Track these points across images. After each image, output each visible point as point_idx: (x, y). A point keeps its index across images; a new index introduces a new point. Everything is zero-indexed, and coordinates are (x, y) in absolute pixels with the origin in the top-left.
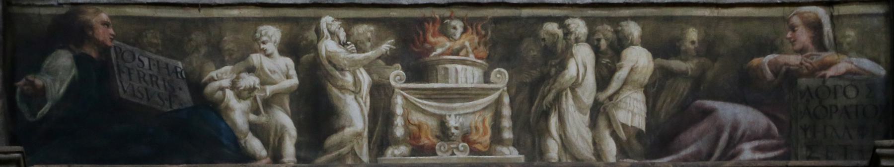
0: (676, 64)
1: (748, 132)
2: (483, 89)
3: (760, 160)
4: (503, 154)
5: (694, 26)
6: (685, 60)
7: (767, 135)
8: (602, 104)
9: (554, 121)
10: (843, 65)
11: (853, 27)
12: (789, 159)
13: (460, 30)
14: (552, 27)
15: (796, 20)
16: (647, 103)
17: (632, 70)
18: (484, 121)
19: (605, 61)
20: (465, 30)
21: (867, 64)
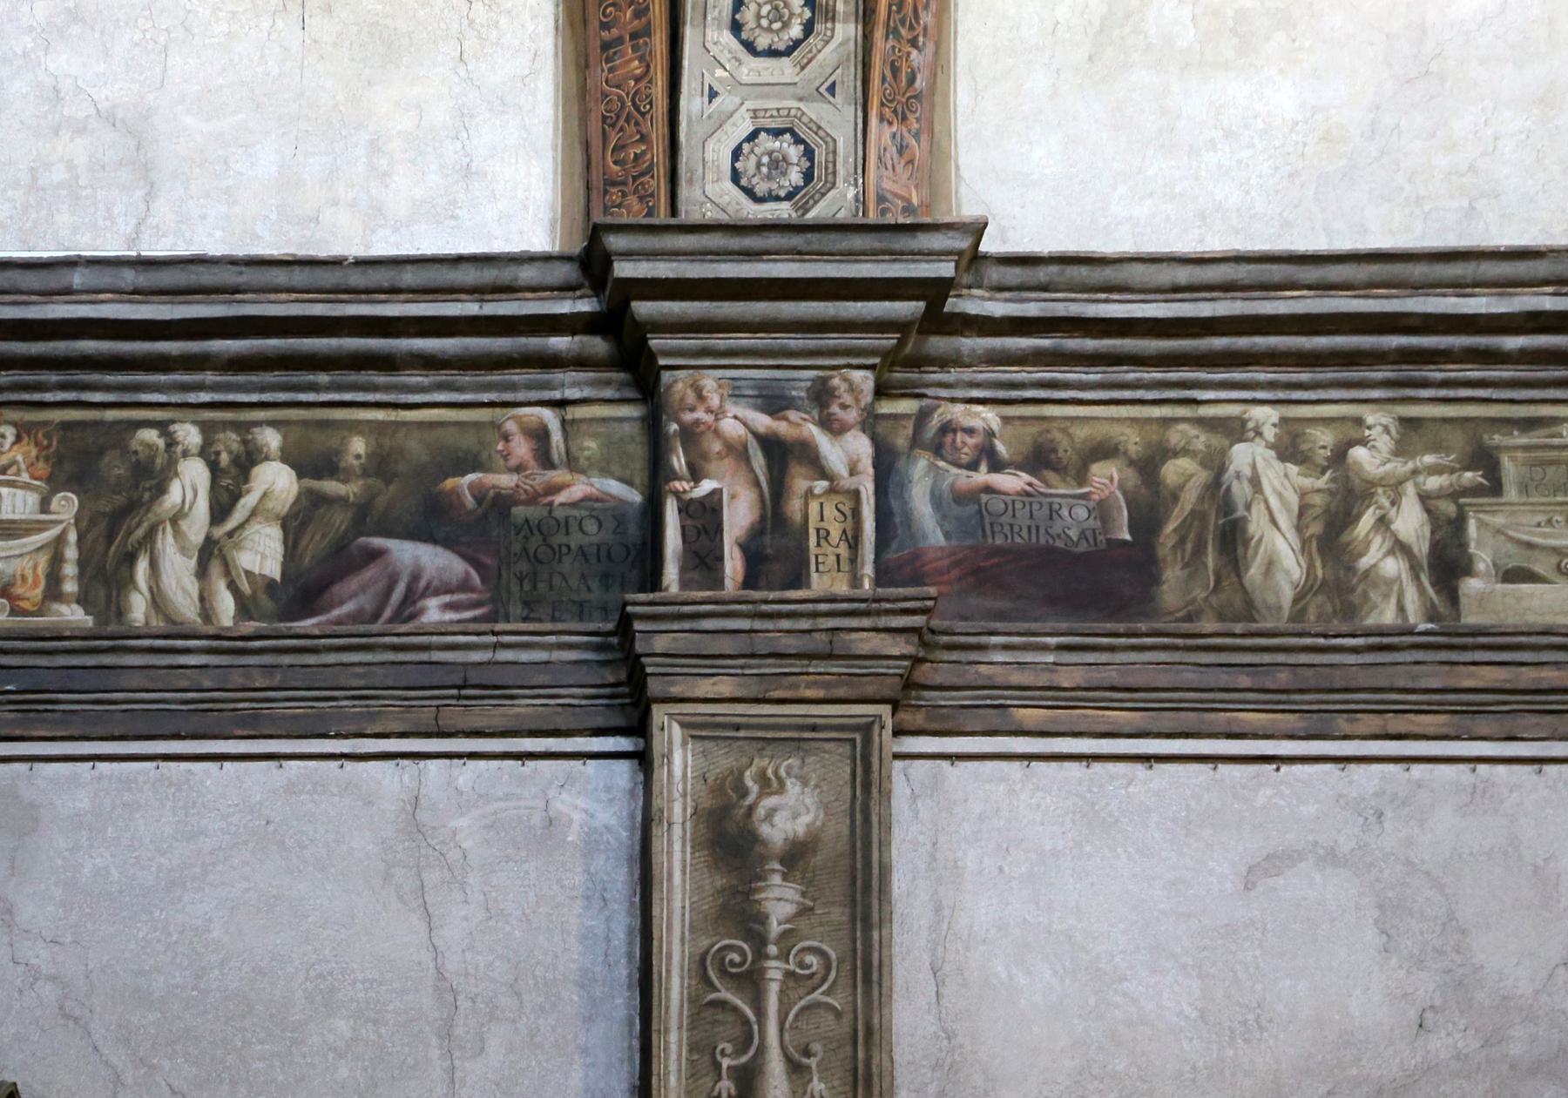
0: (331, 486)
1: (436, 583)
2: (38, 522)
3: (452, 622)
4: (61, 615)
5: (361, 433)
6: (345, 482)
7: (464, 586)
8: (216, 542)
9: (142, 567)
10: (579, 488)
11: (594, 436)
12: (496, 621)
13: (10, 438)
14: (150, 435)
15: (511, 426)
16: (285, 542)
17: (265, 494)
18: (35, 568)
19: (225, 482)
20: (18, 439)
21: (614, 487)
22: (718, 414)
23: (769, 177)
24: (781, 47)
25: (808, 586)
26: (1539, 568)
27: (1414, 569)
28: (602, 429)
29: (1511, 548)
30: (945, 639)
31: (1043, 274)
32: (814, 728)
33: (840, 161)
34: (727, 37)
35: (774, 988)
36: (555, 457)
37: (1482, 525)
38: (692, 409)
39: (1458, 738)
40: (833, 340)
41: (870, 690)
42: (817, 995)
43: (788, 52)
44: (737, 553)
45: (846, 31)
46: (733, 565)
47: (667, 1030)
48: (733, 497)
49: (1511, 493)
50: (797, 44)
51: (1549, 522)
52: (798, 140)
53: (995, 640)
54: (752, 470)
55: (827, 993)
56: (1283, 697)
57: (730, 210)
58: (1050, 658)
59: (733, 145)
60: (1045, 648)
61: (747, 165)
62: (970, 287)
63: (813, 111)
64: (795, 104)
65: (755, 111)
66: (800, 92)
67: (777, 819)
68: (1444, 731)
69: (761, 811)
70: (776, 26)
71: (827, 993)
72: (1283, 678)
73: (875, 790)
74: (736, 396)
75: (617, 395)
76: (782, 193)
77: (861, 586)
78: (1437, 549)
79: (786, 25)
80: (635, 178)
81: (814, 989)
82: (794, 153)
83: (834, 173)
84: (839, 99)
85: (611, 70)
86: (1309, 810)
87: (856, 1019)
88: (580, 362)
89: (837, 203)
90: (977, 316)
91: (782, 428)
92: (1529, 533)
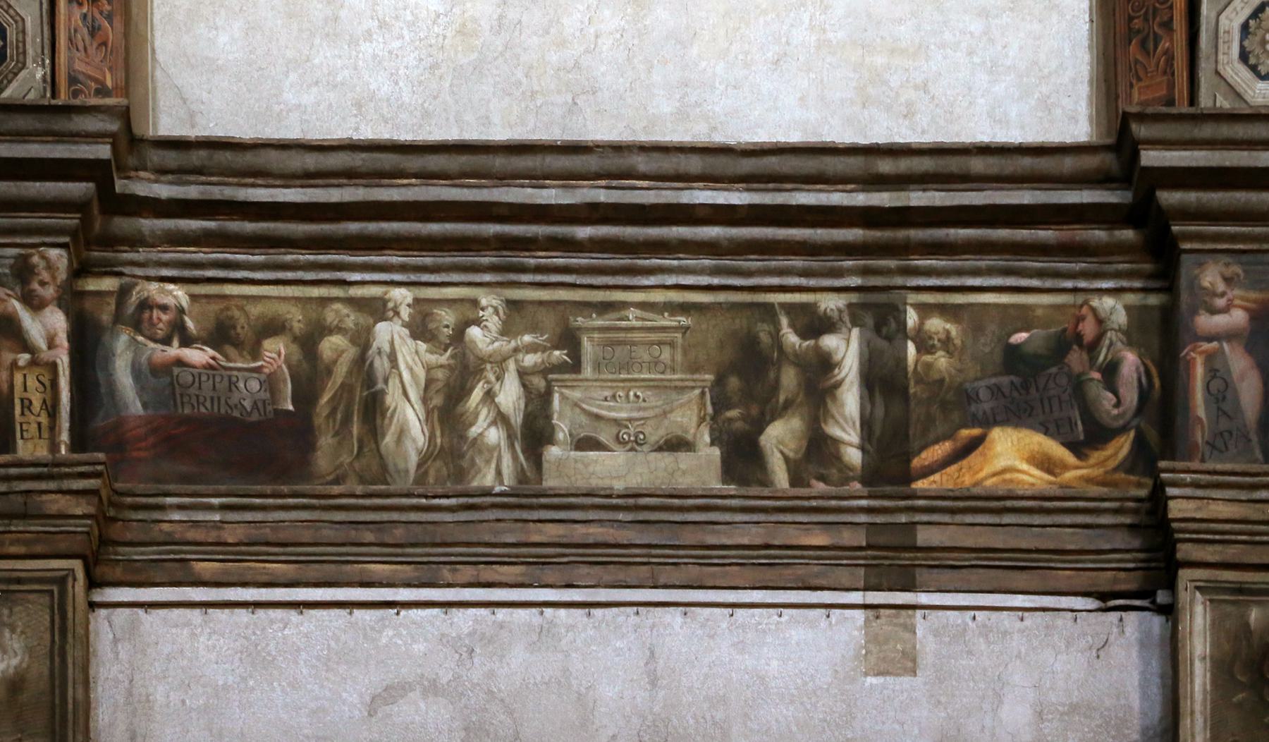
25: (14, 451)
26: (603, 438)
27: (511, 437)
29: (584, 419)
30: (129, 500)
32: (19, 581)
33: (29, 39)
37: (564, 398)
39: (530, 586)
41: (63, 546)
49: (588, 371)
51: (614, 397)
53: (169, 500)
56: (399, 550)
58: (217, 517)
60: (210, 508)
68: (520, 579)
72: (399, 534)
73: (70, 636)
77: (59, 451)
78: (529, 419)
83: (24, 53)
86: (419, 647)
92: (599, 407)
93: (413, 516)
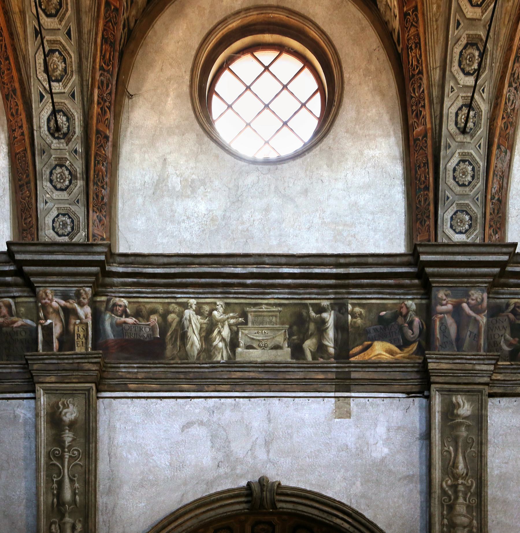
22: (51, 300)
23: (62, 229)
24: (64, 188)
25: (75, 350)
26: (254, 345)
27: (226, 346)
28: (25, 305)
29: (249, 340)
31: (131, 259)
32: (76, 390)
33: (81, 224)
34: (49, 184)
35: (67, 460)
36: (13, 313)
37: (242, 333)
38: (45, 299)
39: (232, 391)
40: (78, 279)
41: (89, 379)
42: (77, 462)
43: (65, 190)
44: (57, 341)
45: (80, 183)
46: (56, 344)
47: (41, 472)
48: (56, 325)
49: (250, 325)
50: (68, 187)
51: (258, 332)
52: (70, 217)
54: (60, 317)
55: (79, 461)
56: (191, 381)
57: (52, 239)
59: (52, 218)
61: (57, 225)
62: (113, 263)
63: (73, 208)
64: (68, 206)
65: (58, 208)
66: (69, 202)
67: (67, 415)
68: (229, 389)
69: (63, 413)
70: (62, 181)
71: (79, 461)
72: (191, 375)
73: (91, 407)
74: (56, 295)
75: (28, 295)
76: (66, 234)
78: (232, 339)
79: (64, 181)
80: (29, 229)
81: (76, 460)
82: (69, 221)
83: (79, 228)
84: (80, 205)
85: (22, 194)
86: (197, 411)
87: (86, 467)
88: (16, 285)
89: (80, 237)
90: (115, 272)
91: (68, 304)
92: (253, 336)
93: (196, 370)
